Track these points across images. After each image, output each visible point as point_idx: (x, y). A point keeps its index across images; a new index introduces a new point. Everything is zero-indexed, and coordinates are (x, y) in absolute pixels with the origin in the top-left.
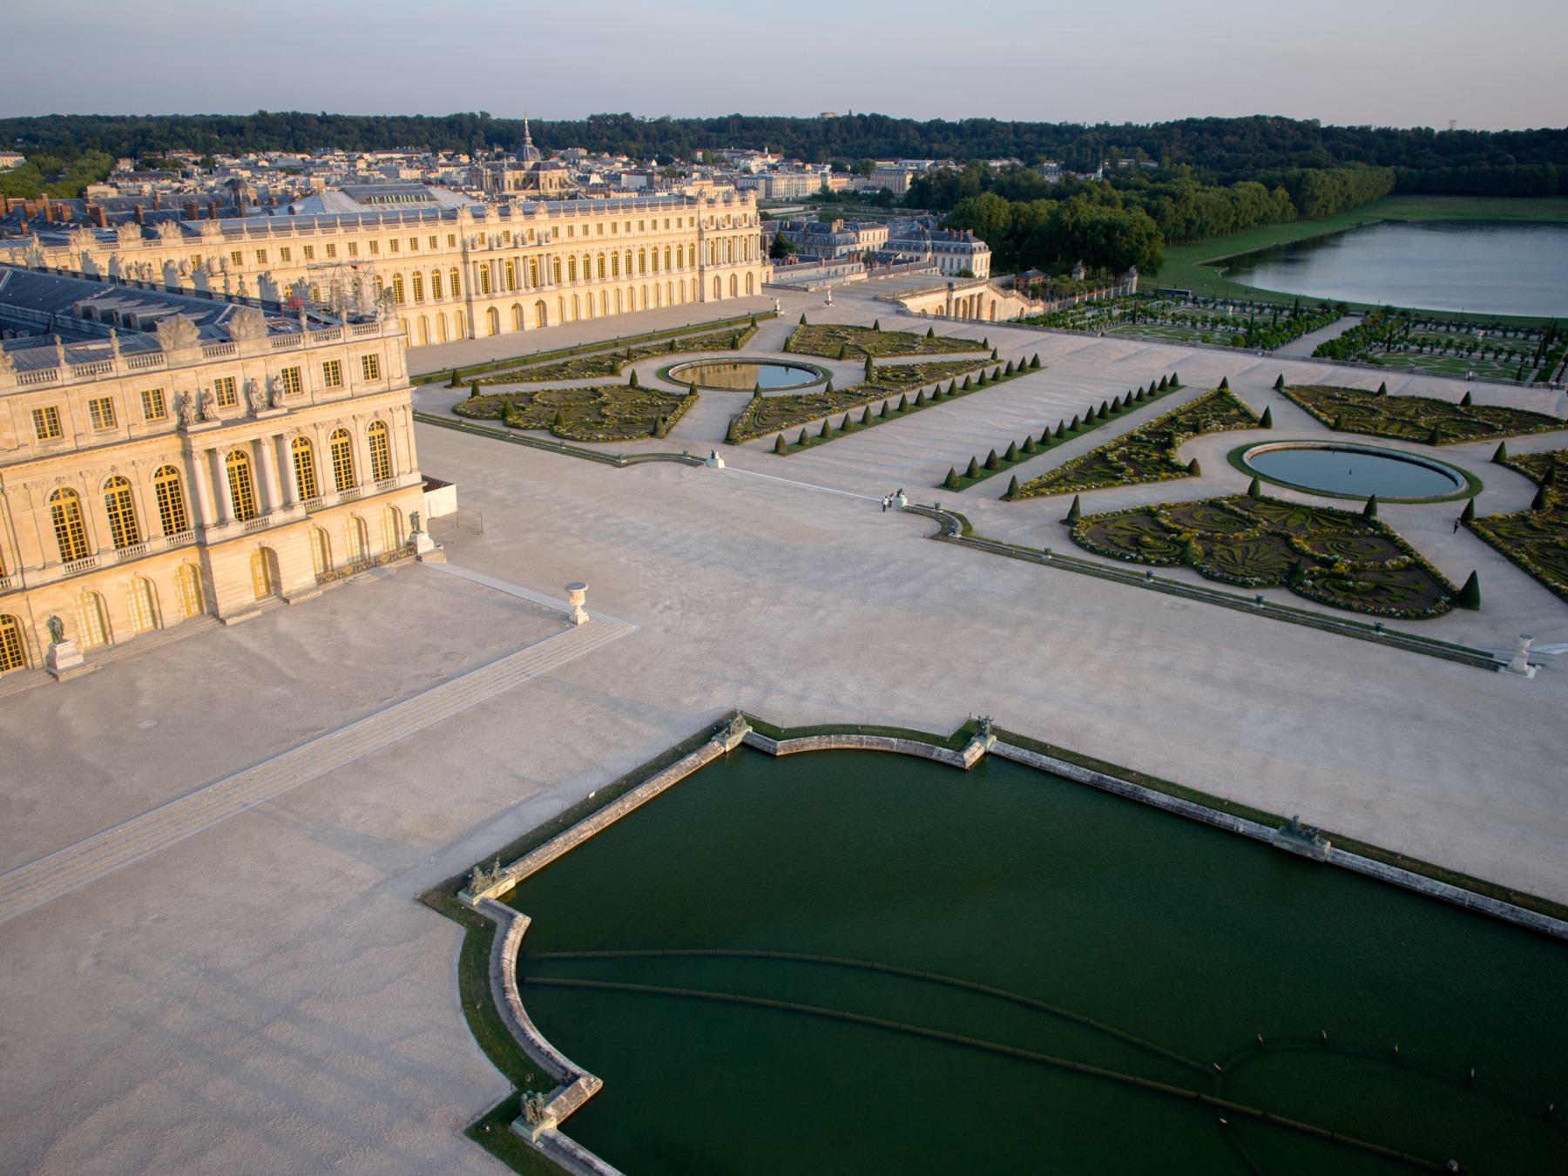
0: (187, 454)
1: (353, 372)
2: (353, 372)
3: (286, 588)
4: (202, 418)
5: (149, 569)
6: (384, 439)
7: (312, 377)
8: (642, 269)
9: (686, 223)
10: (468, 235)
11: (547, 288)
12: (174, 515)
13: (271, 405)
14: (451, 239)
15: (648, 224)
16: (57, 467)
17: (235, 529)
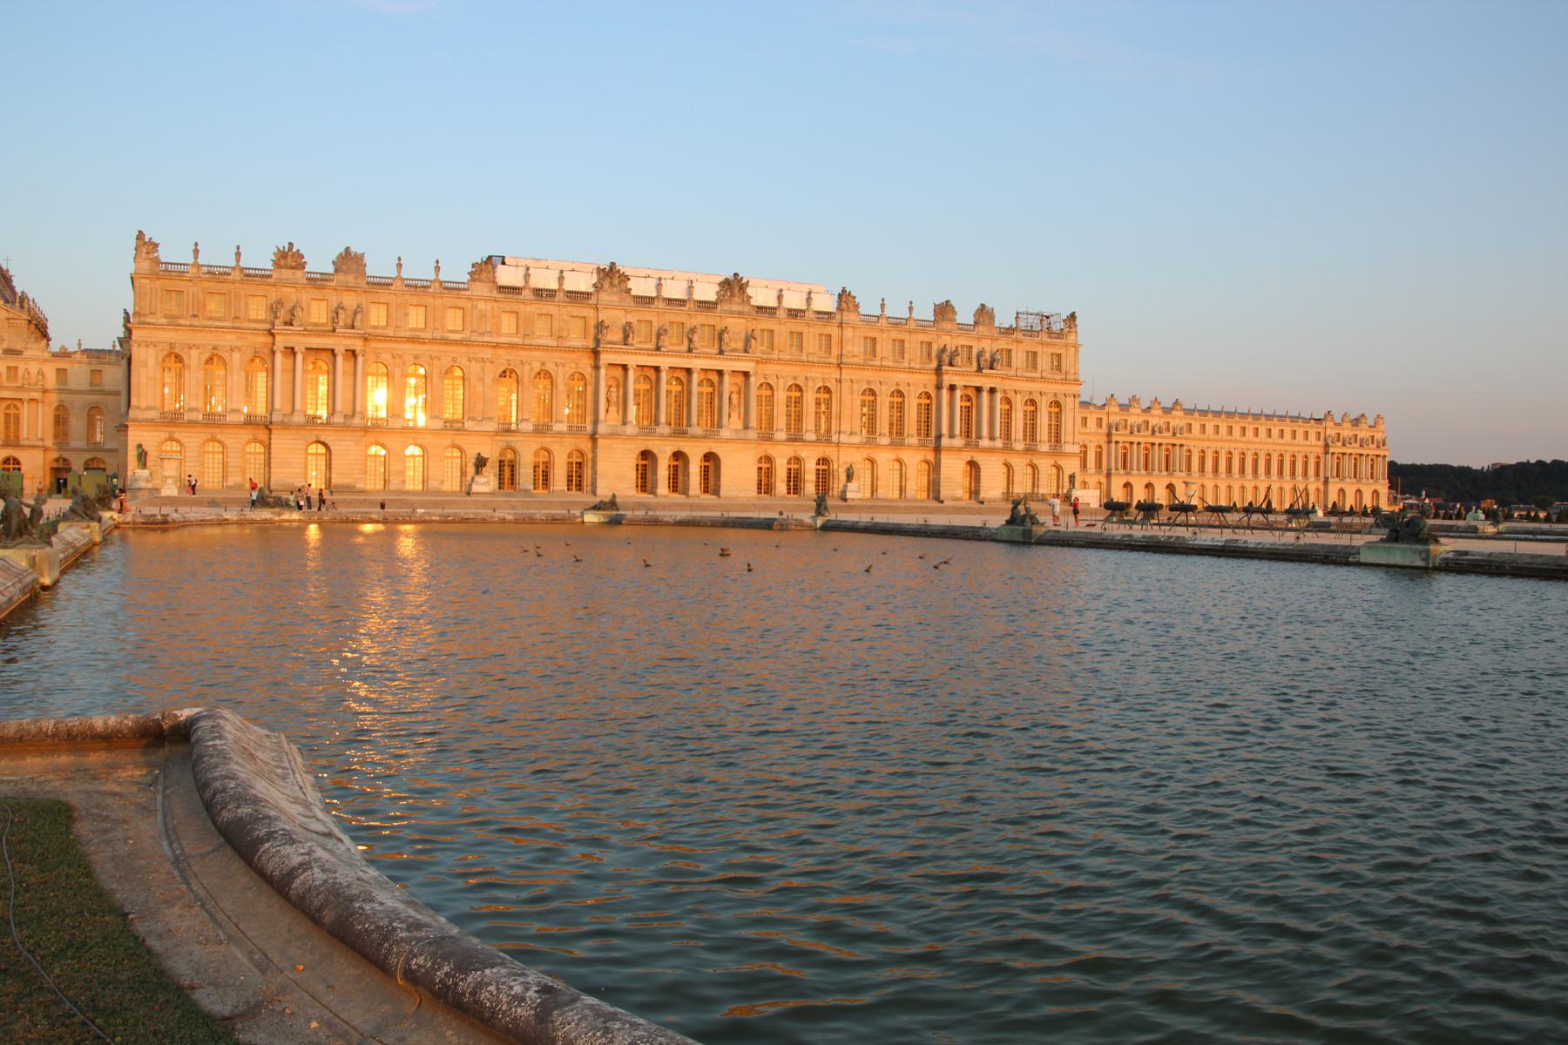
0: (939, 387)
1: (1044, 362)
2: (1044, 362)
3: (982, 495)
4: (951, 364)
5: (905, 456)
7: (1019, 358)
8: (1268, 472)
9: (1312, 436)
10: (1114, 419)
11: (1177, 473)
13: (992, 368)
14: (1100, 420)
15: (1275, 432)
16: (869, 375)
17: (958, 442)
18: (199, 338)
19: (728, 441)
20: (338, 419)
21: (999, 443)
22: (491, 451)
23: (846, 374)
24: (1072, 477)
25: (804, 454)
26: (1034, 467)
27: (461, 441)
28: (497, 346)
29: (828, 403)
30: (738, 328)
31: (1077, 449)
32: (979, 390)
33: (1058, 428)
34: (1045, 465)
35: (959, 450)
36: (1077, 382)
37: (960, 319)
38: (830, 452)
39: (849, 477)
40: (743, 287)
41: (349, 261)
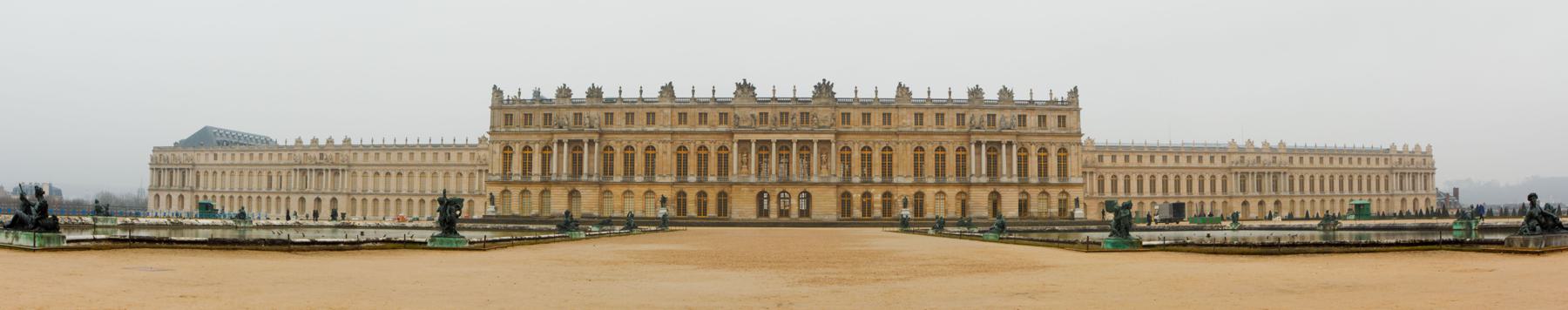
5: (946, 190)
6: (1065, 159)
12: (961, 169)
16: (919, 138)
18: (518, 138)
20: (584, 178)
21: (1015, 180)
22: (669, 193)
23: (901, 139)
24: (1077, 200)
25: (872, 191)
26: (1044, 192)
27: (653, 189)
28: (673, 133)
29: (891, 157)
30: (824, 114)
32: (1000, 144)
33: (1065, 167)
35: (984, 185)
36: (1079, 135)
37: (986, 97)
38: (890, 189)
39: (905, 206)
41: (595, 93)
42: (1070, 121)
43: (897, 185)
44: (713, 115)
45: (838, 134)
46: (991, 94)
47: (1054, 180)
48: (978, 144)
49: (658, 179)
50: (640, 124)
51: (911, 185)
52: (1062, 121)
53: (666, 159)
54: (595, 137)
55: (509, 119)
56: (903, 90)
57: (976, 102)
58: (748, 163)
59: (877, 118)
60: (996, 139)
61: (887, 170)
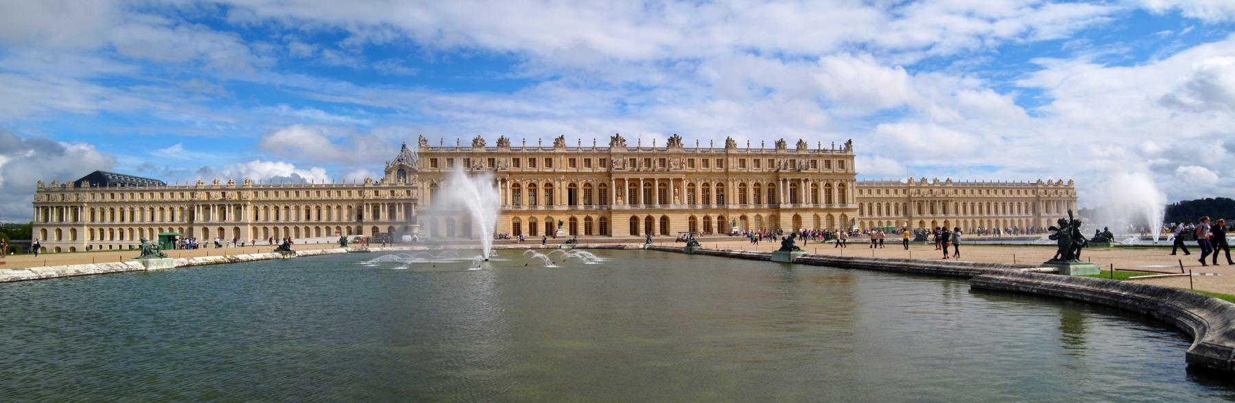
17: (789, 206)
19: (673, 211)
21: (811, 206)
24: (853, 220)
31: (856, 206)
32: (799, 181)
34: (837, 216)
40: (678, 141)
42: (848, 163)
43: (728, 210)
44: (595, 161)
45: (687, 174)
46: (791, 145)
47: (837, 206)
48: (785, 181)
49: (556, 208)
50: (541, 166)
51: (738, 211)
52: (842, 164)
53: (561, 193)
54: (507, 177)
55: (434, 163)
56: (729, 142)
57: (782, 152)
58: (623, 195)
59: (713, 162)
60: (797, 177)
61: (721, 199)
